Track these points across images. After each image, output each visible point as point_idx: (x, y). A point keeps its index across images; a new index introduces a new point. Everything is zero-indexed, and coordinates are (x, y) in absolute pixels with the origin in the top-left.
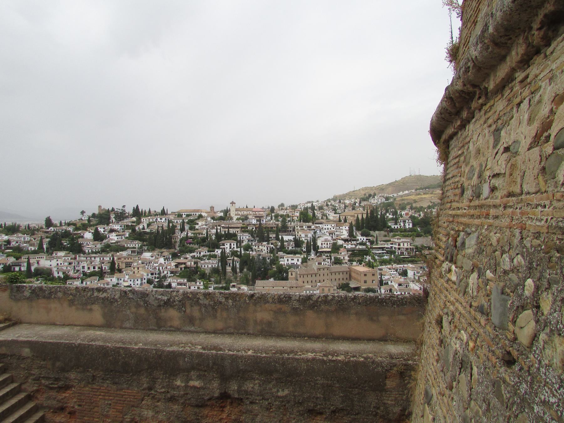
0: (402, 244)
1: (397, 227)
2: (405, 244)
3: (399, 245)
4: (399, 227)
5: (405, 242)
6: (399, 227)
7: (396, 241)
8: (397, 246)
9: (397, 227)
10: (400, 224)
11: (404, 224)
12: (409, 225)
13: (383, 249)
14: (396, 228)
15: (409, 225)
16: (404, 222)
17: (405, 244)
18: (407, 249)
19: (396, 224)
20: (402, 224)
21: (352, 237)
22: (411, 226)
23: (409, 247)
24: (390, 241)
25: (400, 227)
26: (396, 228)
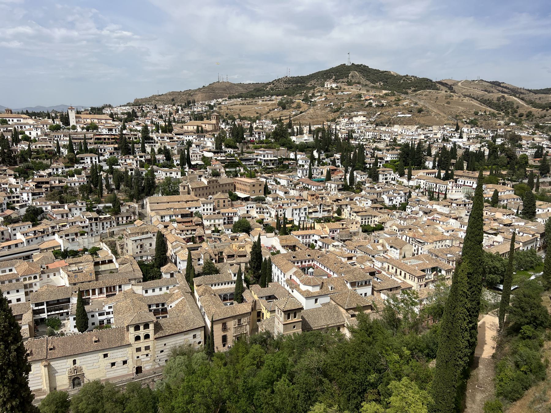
0: (266, 156)
1: (253, 139)
2: (269, 155)
3: (264, 157)
4: (254, 139)
5: (269, 154)
6: (254, 139)
7: (261, 153)
8: (262, 158)
9: (253, 139)
10: (255, 136)
11: (259, 136)
12: (263, 137)
13: (249, 160)
14: (252, 139)
15: (263, 137)
16: (259, 133)
17: (269, 155)
18: (272, 160)
19: (251, 136)
20: (257, 136)
21: (218, 150)
22: (264, 138)
23: (272, 158)
24: (254, 153)
25: (256, 139)
26: (252, 139)
